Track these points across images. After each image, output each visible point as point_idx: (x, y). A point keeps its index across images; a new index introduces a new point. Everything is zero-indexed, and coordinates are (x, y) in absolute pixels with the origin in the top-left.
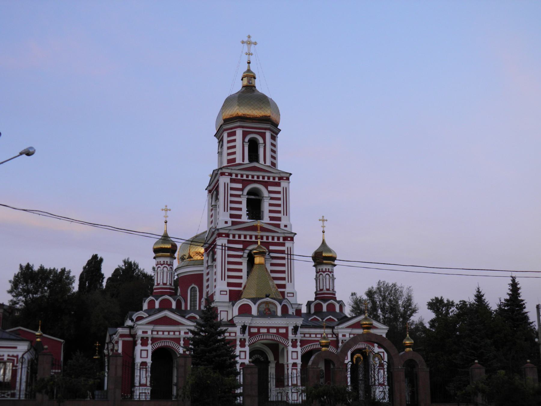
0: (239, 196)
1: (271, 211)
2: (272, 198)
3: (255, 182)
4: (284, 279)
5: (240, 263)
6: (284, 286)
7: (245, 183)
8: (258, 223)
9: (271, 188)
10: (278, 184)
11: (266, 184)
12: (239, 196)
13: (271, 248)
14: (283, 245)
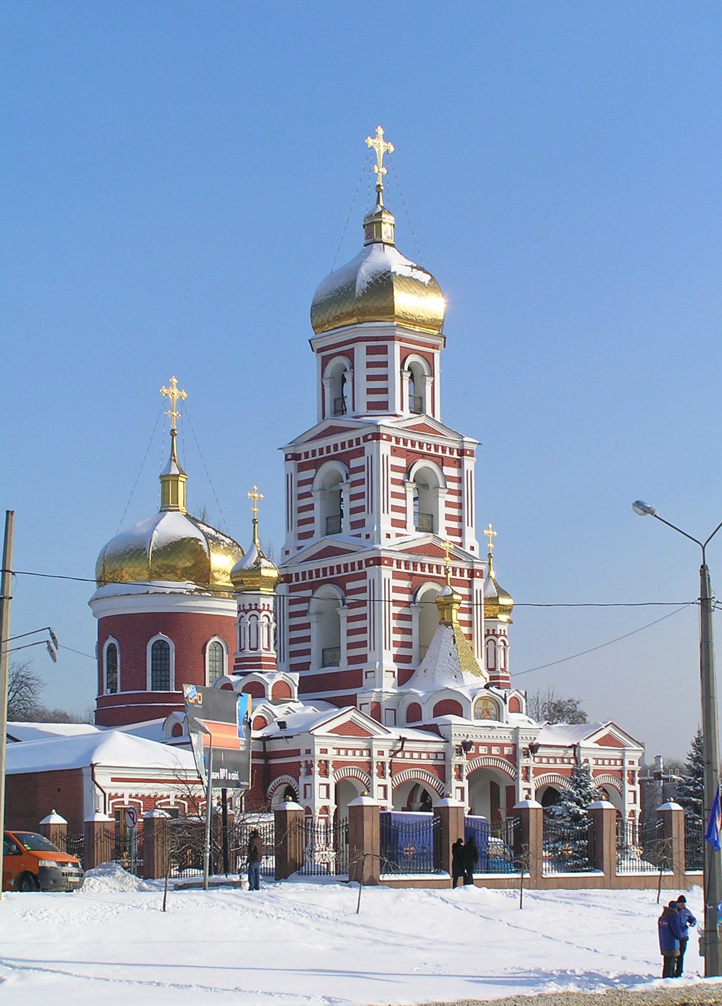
0: (308, 495)
1: (353, 511)
2: (354, 484)
3: (333, 458)
4: (363, 644)
5: (307, 626)
6: (363, 659)
7: (316, 465)
8: (333, 541)
9: (354, 463)
10: (361, 452)
11: (344, 458)
12: (308, 495)
13: (350, 586)
14: (364, 576)
